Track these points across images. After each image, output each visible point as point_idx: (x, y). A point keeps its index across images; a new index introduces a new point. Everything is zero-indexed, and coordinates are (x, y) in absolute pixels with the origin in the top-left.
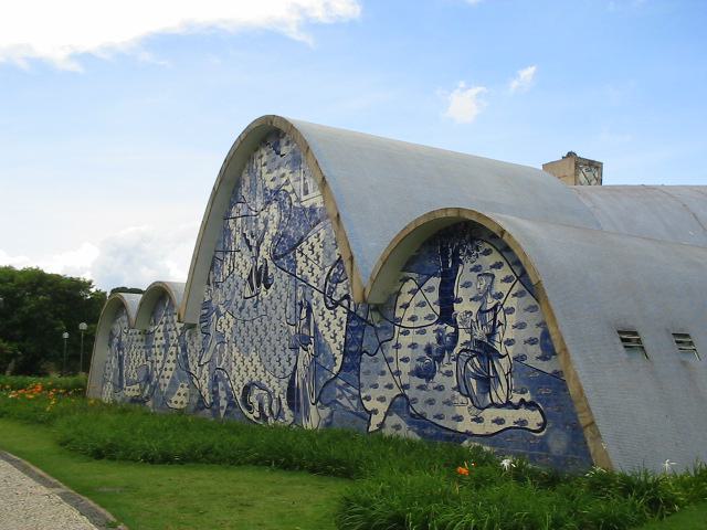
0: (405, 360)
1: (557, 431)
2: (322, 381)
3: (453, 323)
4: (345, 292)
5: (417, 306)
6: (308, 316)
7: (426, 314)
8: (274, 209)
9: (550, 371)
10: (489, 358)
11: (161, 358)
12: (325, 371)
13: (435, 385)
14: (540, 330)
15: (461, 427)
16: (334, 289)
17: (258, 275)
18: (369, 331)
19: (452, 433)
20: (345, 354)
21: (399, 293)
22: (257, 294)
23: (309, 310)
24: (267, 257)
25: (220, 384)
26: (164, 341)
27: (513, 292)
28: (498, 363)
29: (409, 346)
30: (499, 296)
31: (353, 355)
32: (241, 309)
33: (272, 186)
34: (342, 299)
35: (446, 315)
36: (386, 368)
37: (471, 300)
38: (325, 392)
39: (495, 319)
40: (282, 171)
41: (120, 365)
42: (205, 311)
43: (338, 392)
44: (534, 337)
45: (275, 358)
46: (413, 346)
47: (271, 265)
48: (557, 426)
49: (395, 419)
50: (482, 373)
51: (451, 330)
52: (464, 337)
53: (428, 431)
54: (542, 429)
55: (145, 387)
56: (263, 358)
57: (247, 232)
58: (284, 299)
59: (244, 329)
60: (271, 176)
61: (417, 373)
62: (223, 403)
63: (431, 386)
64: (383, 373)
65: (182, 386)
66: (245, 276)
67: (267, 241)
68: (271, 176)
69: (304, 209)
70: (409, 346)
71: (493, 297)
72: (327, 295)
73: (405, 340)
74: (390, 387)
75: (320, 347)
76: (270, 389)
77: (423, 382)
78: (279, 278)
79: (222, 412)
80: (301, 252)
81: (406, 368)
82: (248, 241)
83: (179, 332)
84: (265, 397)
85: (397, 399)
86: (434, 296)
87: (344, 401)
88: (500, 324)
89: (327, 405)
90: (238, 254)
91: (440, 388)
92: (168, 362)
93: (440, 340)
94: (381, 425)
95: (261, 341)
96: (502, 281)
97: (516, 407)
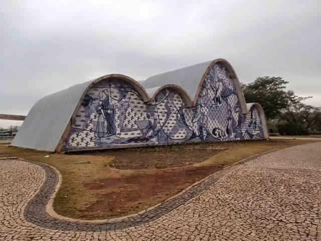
8: (221, 83)
11: (165, 118)
17: (217, 99)
23: (231, 112)
25: (203, 129)
26: (166, 111)
31: (240, 122)
33: (221, 78)
35: (252, 118)
41: (109, 118)
45: (223, 122)
49: (246, 134)
55: (148, 132)
59: (212, 114)
61: (249, 126)
62: (205, 134)
65: (182, 130)
66: (212, 98)
72: (235, 110)
73: (247, 121)
78: (224, 103)
79: (205, 137)
81: (247, 125)
83: (178, 109)
92: (171, 120)
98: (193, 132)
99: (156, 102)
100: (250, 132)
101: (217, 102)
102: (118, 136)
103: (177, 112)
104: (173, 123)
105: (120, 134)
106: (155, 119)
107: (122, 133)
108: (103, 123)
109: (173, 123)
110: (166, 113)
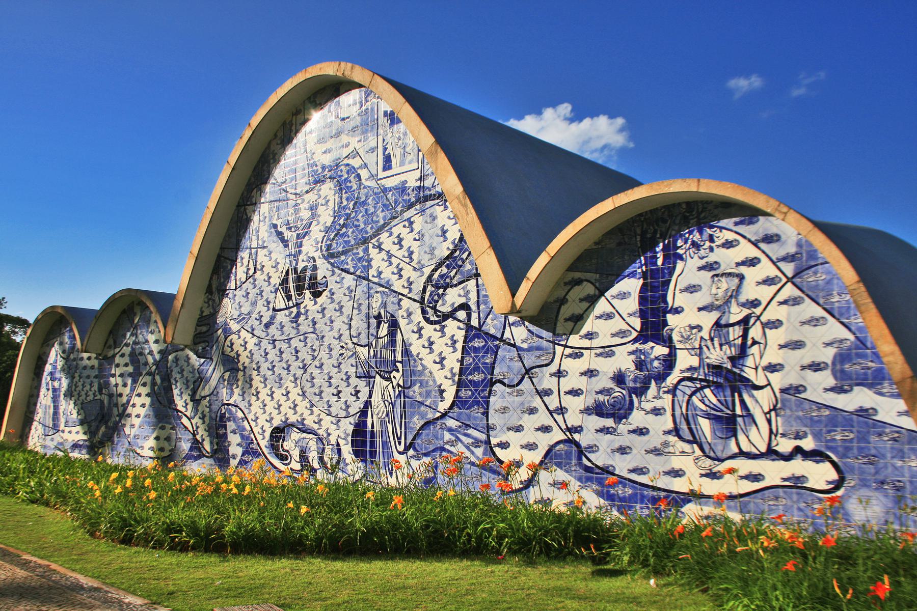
0: (575, 393)
1: (865, 492)
2: (417, 422)
3: (668, 341)
4: (463, 300)
5: (598, 318)
6: (392, 334)
7: (614, 331)
9: (851, 408)
10: (734, 390)
12: (423, 408)
13: (631, 428)
14: (831, 352)
15: (679, 485)
16: (440, 297)
17: (299, 279)
18: (504, 352)
19: (662, 494)
20: (460, 385)
21: (563, 301)
22: (298, 305)
23: (394, 324)
24: (317, 255)
25: (231, 425)
26: (130, 369)
27: (781, 297)
28: (752, 396)
29: (582, 374)
30: (755, 303)
32: (267, 326)
33: (327, 160)
34: (455, 310)
36: (537, 402)
37: (700, 309)
38: (423, 436)
39: (745, 336)
40: (344, 139)
42: (204, 329)
43: (448, 436)
44: (818, 360)
45: (328, 392)
46: (590, 373)
47: (320, 262)
48: (864, 484)
50: (722, 411)
51: (661, 350)
52: (685, 360)
53: (620, 491)
54: (837, 488)
55: (98, 428)
56: (309, 391)
57: (279, 223)
58: (347, 310)
60: (324, 147)
63: (622, 428)
64: (532, 411)
66: (276, 280)
67: (317, 233)
68: (324, 147)
69: (385, 190)
70: (582, 374)
71: (743, 305)
74: (546, 429)
75: (413, 374)
76: (320, 432)
77: (609, 422)
80: (379, 247)
81: (574, 404)
82: (280, 234)
83: (158, 357)
84: (313, 445)
85: (562, 445)
86: (632, 304)
87: (460, 448)
88: (755, 343)
89: (425, 455)
90: (261, 252)
91: (641, 432)
92: (139, 395)
93: (640, 365)
94: (529, 484)
95: (305, 368)
96: (759, 283)
97: (787, 458)
98: (194, 435)
99: (115, 348)
100: (622, 465)
101: (299, 289)
102: (61, 434)
103: (154, 367)
104: (143, 405)
105: (63, 431)
106: (111, 396)
107: (67, 429)
108: (50, 407)
109: (143, 405)
110: (130, 375)
